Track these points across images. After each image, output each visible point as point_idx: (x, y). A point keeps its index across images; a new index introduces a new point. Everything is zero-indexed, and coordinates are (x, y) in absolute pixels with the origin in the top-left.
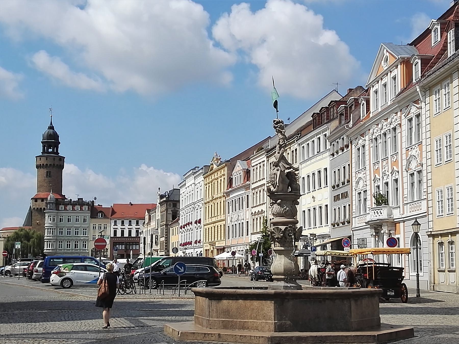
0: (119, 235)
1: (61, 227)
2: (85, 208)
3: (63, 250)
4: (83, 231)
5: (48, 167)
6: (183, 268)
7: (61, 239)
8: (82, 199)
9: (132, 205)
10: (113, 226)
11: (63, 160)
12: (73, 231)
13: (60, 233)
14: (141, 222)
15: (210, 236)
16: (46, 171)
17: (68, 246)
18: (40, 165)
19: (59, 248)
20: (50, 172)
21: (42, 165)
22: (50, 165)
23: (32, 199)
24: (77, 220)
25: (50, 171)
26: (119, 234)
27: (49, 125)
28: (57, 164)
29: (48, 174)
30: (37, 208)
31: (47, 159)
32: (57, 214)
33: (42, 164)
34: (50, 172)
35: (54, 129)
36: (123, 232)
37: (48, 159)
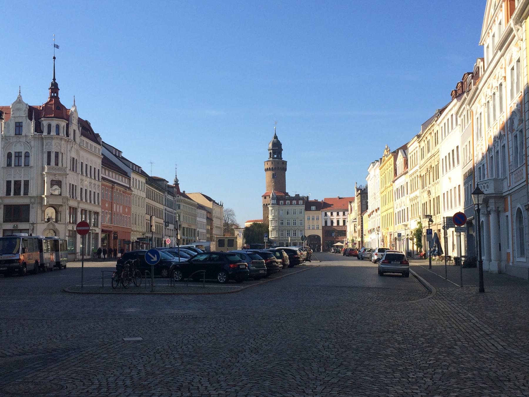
2: (301, 202)
4: (299, 221)
6: (156, 255)
8: (299, 195)
9: (340, 198)
10: (323, 217)
11: (285, 164)
14: (346, 213)
15: (150, 210)
18: (268, 168)
24: (295, 213)
26: (329, 224)
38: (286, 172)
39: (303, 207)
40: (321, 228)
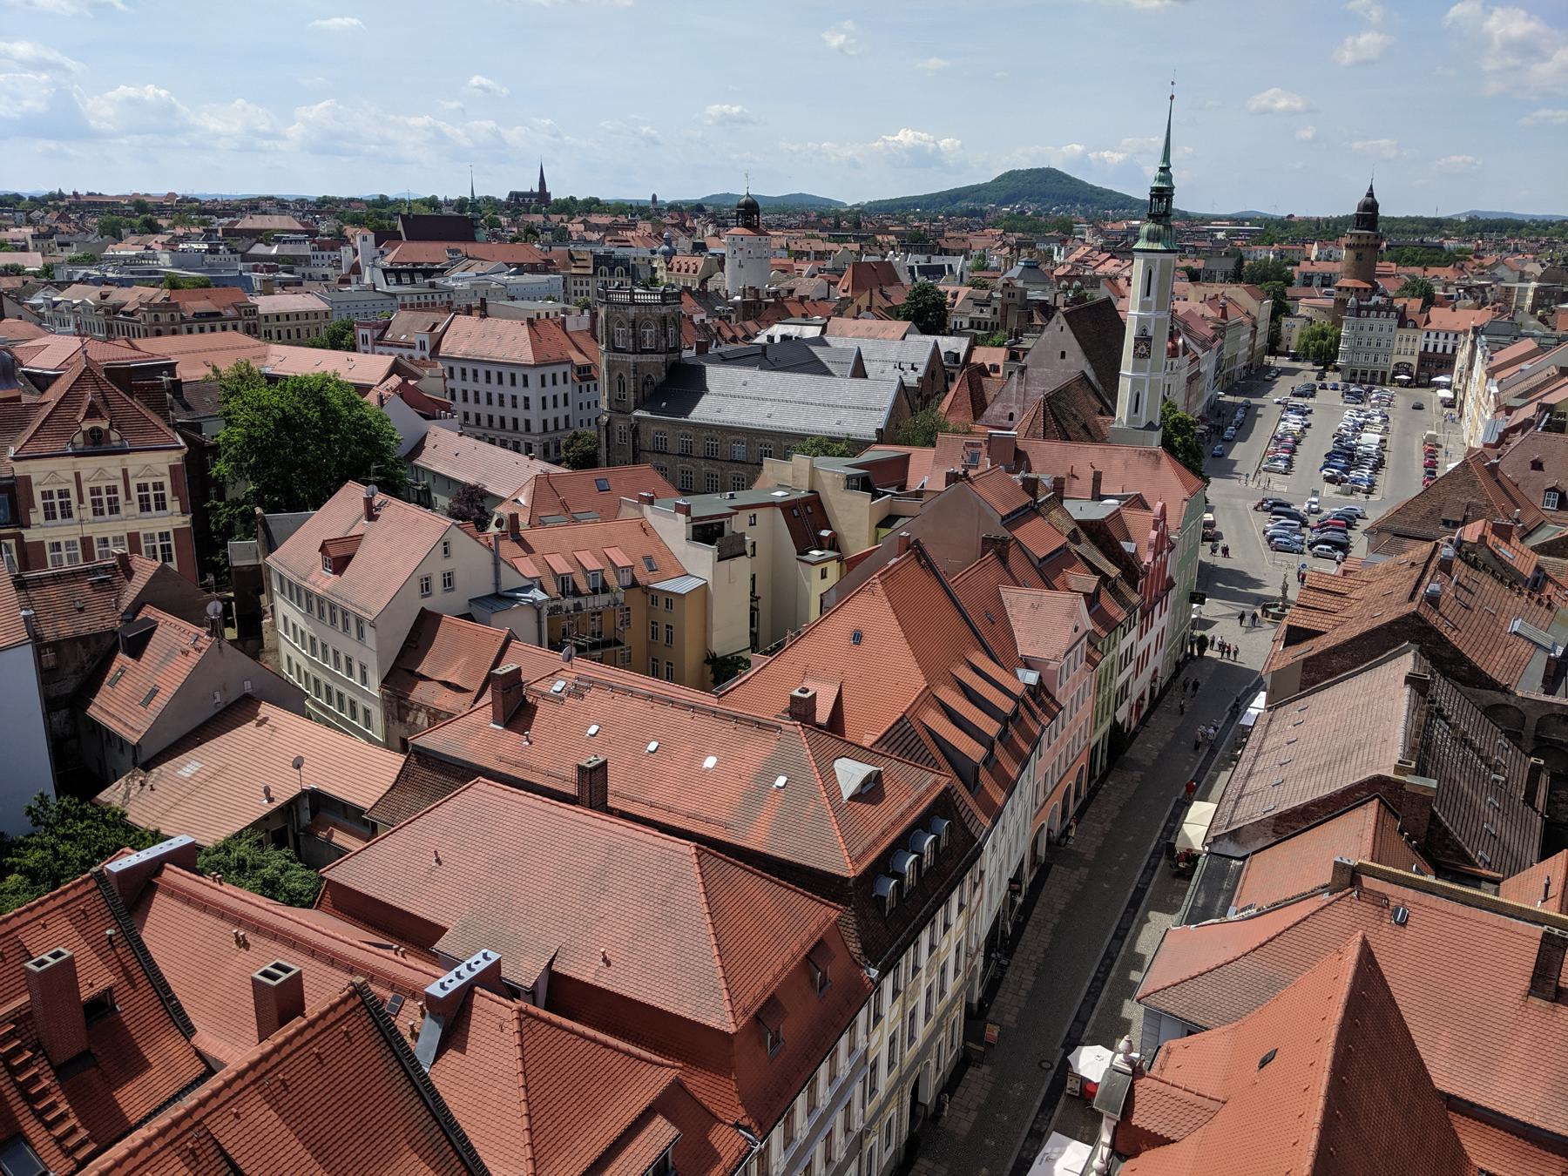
0: (1430, 349)
12: (1374, 342)
17: (1367, 358)
26: (1430, 349)
27: (1367, 190)
29: (1359, 257)
36: (1435, 347)
39: (1395, 322)
40: (1417, 353)
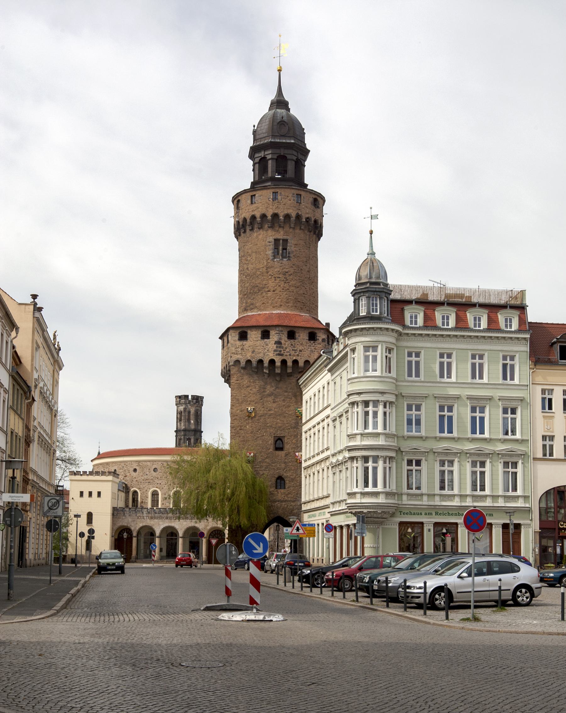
1: (415, 397)
3: (425, 498)
5: (280, 227)
7: (415, 451)
13: (409, 422)
16: (271, 239)
18: (253, 217)
19: (409, 487)
20: (285, 241)
21: (258, 219)
22: (287, 217)
23: (231, 332)
25: (285, 237)
27: (273, 96)
28: (307, 216)
30: (249, 362)
31: (275, 199)
32: (397, 340)
33: (258, 215)
34: (285, 241)
35: (288, 110)
37: (279, 197)
38: (320, 243)
